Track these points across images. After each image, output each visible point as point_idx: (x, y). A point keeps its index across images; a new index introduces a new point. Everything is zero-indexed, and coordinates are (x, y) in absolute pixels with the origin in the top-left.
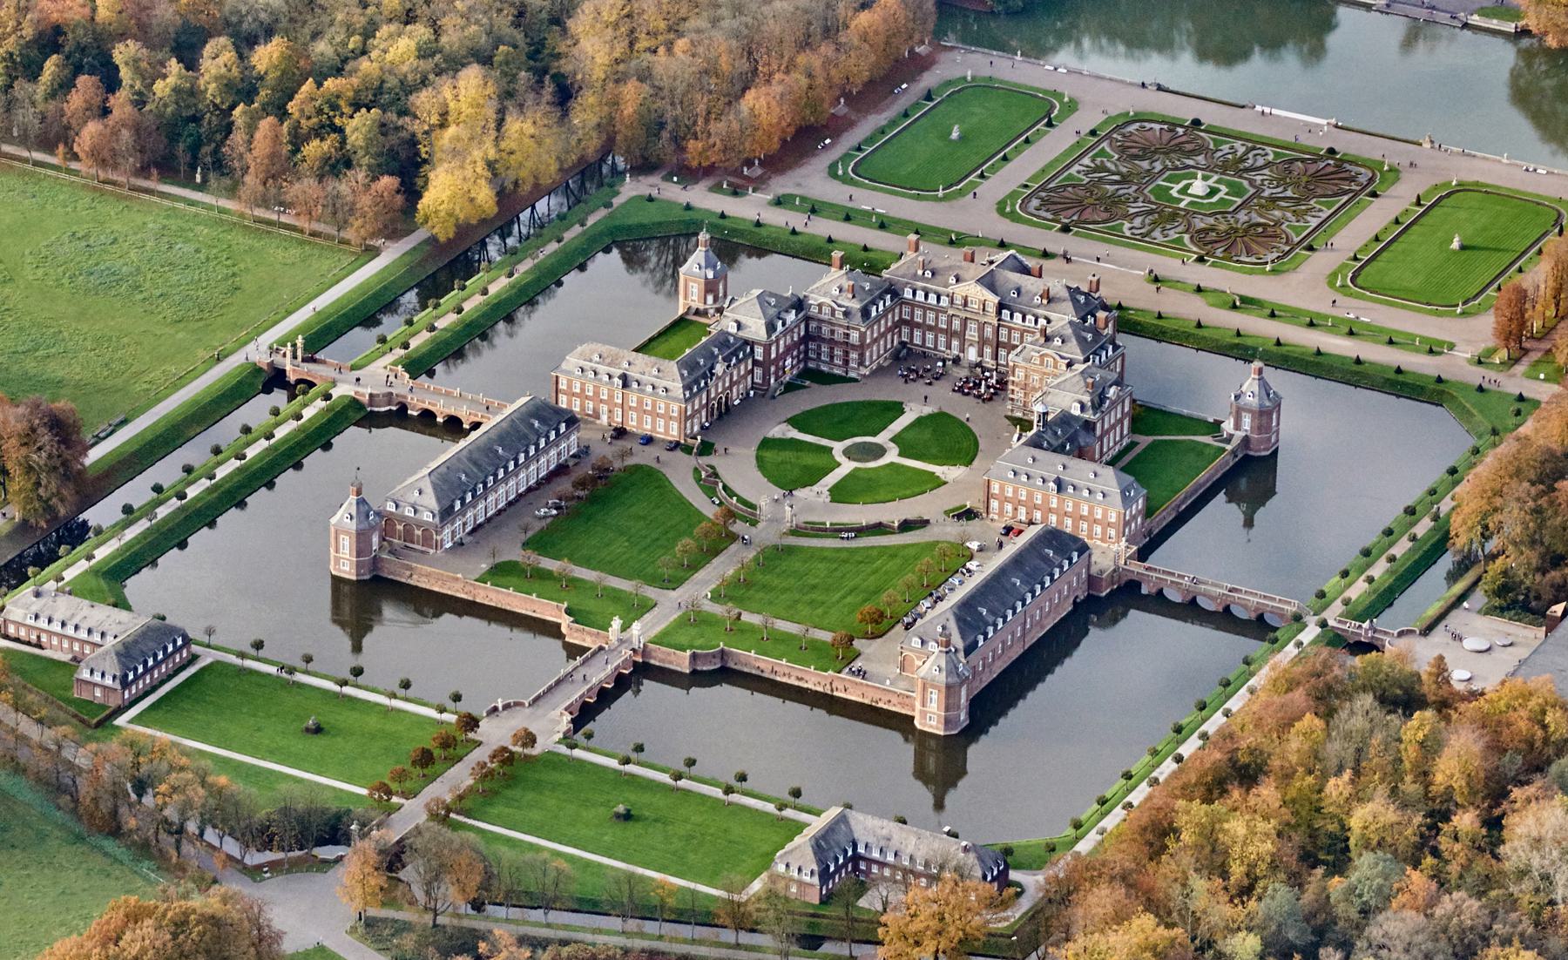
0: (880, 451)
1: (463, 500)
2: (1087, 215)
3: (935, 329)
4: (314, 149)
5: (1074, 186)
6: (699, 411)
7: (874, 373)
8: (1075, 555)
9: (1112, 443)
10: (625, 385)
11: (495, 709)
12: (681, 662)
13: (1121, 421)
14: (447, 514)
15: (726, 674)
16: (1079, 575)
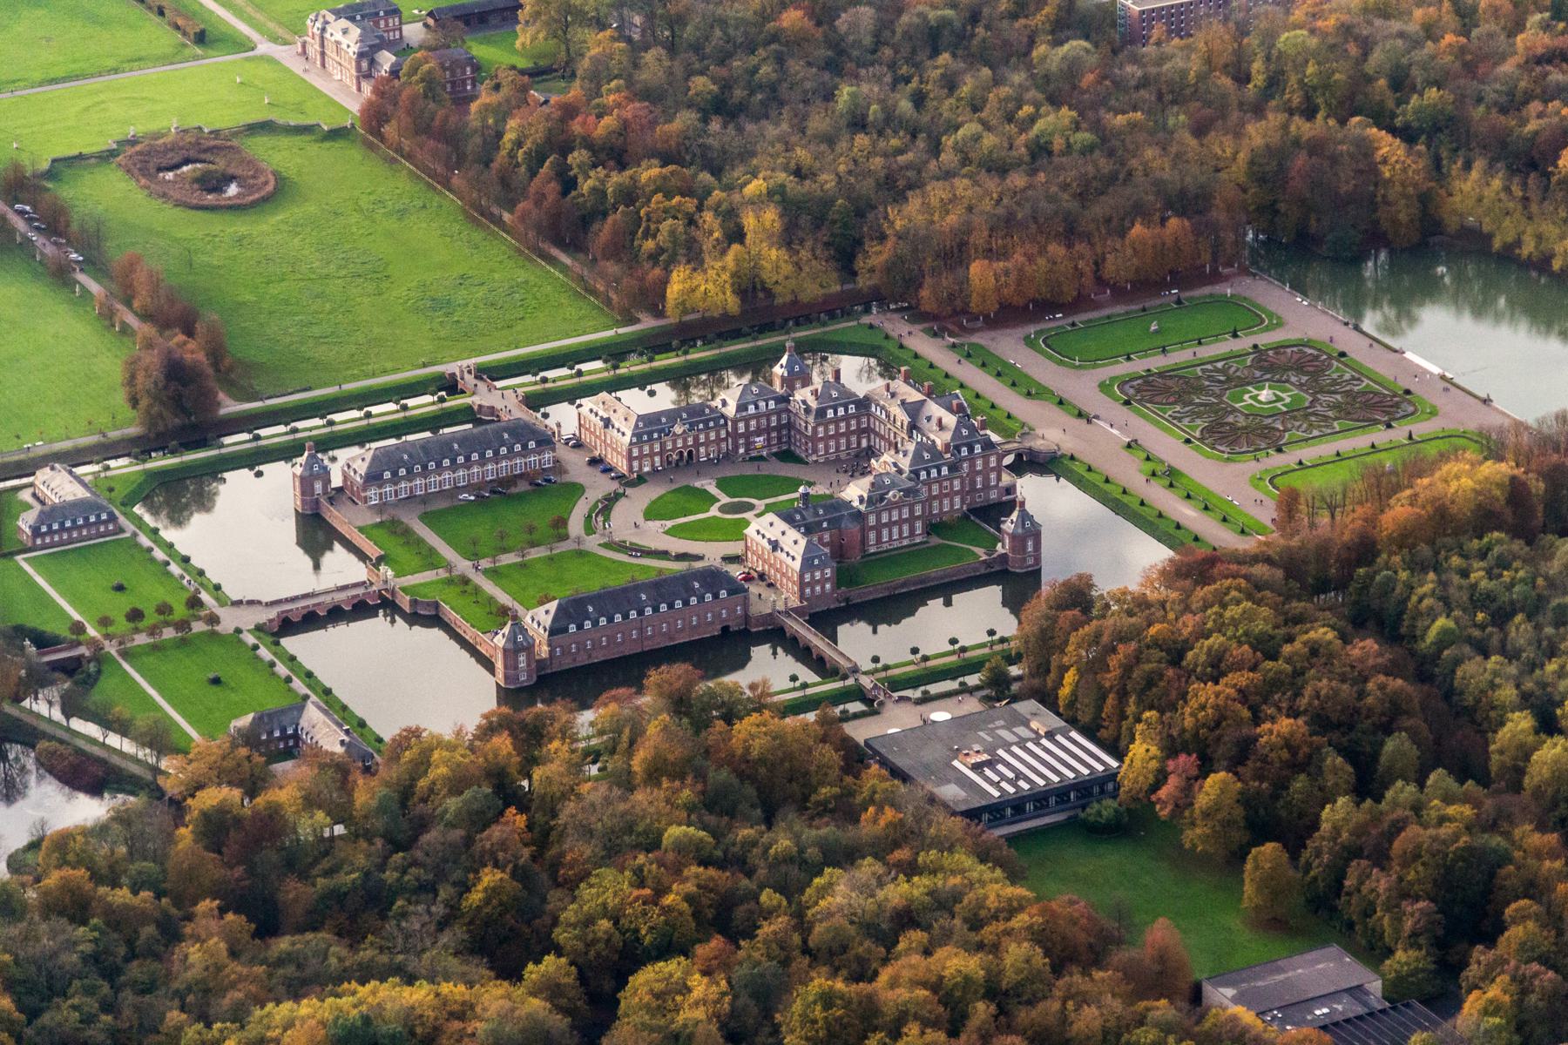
0: (751, 507)
1: (395, 474)
2: (1157, 399)
3: (882, 437)
4: (650, 245)
5: (1181, 377)
6: (652, 455)
7: (827, 462)
8: (723, 594)
9: (895, 538)
10: (606, 426)
11: (239, 603)
12: (404, 602)
13: (912, 520)
14: (373, 478)
15: (434, 619)
16: (732, 611)
